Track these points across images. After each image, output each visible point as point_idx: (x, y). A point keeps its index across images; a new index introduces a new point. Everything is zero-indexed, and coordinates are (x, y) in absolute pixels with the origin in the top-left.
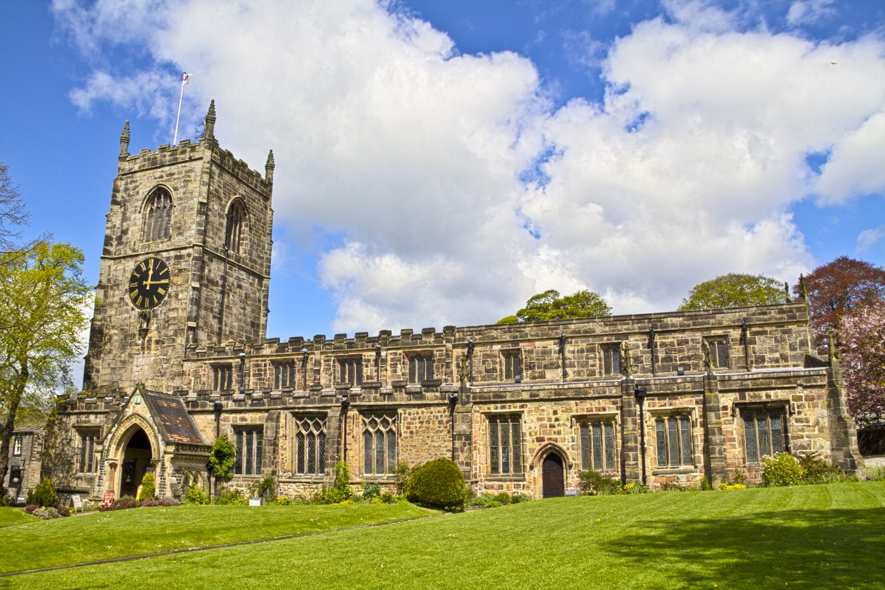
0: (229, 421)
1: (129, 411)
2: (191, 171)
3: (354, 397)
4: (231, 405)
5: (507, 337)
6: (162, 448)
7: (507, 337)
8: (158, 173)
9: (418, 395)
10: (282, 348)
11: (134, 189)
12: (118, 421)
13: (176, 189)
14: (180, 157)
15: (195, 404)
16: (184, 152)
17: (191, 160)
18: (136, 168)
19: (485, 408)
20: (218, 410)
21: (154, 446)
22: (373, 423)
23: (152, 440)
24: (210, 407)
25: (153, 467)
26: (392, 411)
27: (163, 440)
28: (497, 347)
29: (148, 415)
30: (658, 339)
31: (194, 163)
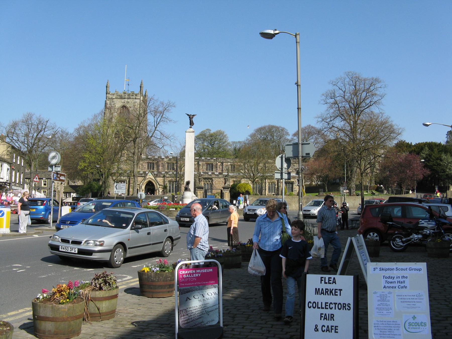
0: (167, 180)
1: (148, 177)
2: (136, 102)
3: (202, 175)
4: (168, 176)
5: (232, 161)
6: (158, 186)
7: (232, 161)
8: (123, 100)
9: (217, 175)
10: (170, 159)
11: (114, 104)
12: (144, 180)
13: (130, 107)
14: (132, 97)
15: (157, 175)
16: (133, 96)
17: (136, 99)
18: (114, 97)
19: (233, 179)
20: (164, 176)
21: (156, 186)
22: (206, 181)
23: (155, 184)
24: (162, 176)
25: (156, 191)
26: (211, 179)
27: (159, 184)
28: (229, 164)
29: (153, 178)
30: (267, 165)
31: (137, 100)
